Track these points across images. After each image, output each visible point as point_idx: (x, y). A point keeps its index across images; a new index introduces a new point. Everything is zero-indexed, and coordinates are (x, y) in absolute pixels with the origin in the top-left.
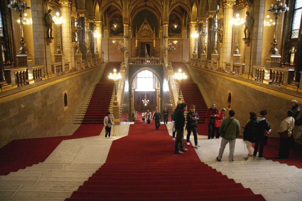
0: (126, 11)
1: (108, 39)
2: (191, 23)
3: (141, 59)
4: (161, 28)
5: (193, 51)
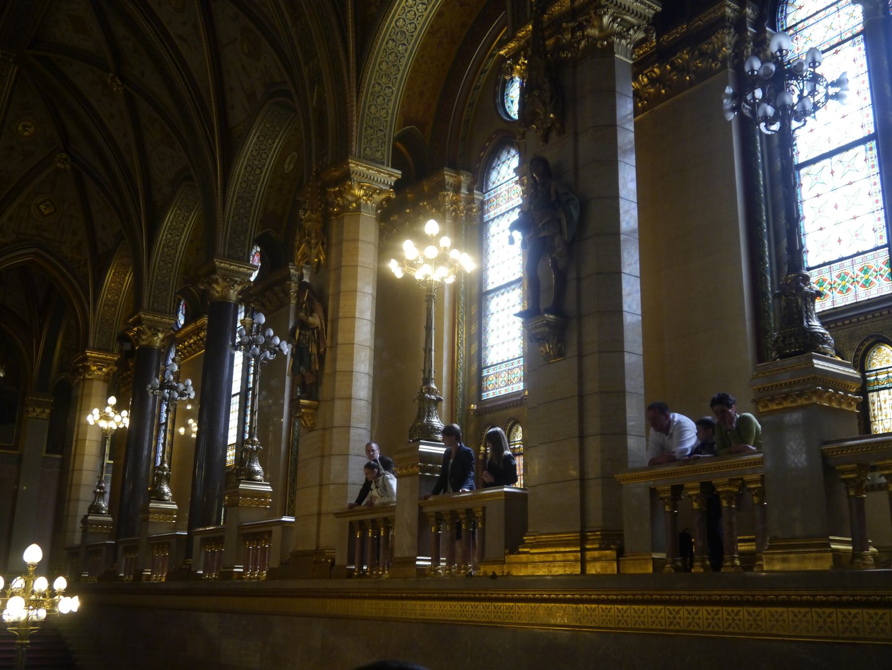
2: (86, 359)
5: (82, 509)
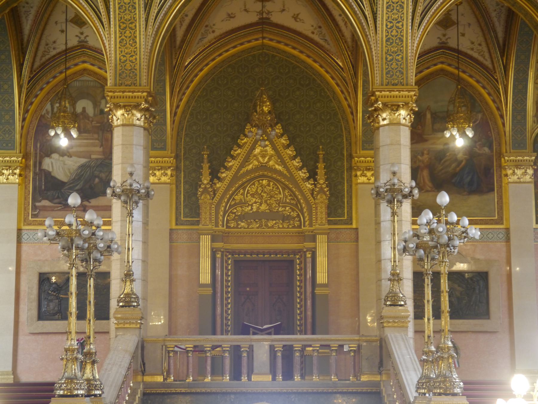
0: (126, 26)
1: (19, 231)
3: (226, 345)
4: (361, 157)
